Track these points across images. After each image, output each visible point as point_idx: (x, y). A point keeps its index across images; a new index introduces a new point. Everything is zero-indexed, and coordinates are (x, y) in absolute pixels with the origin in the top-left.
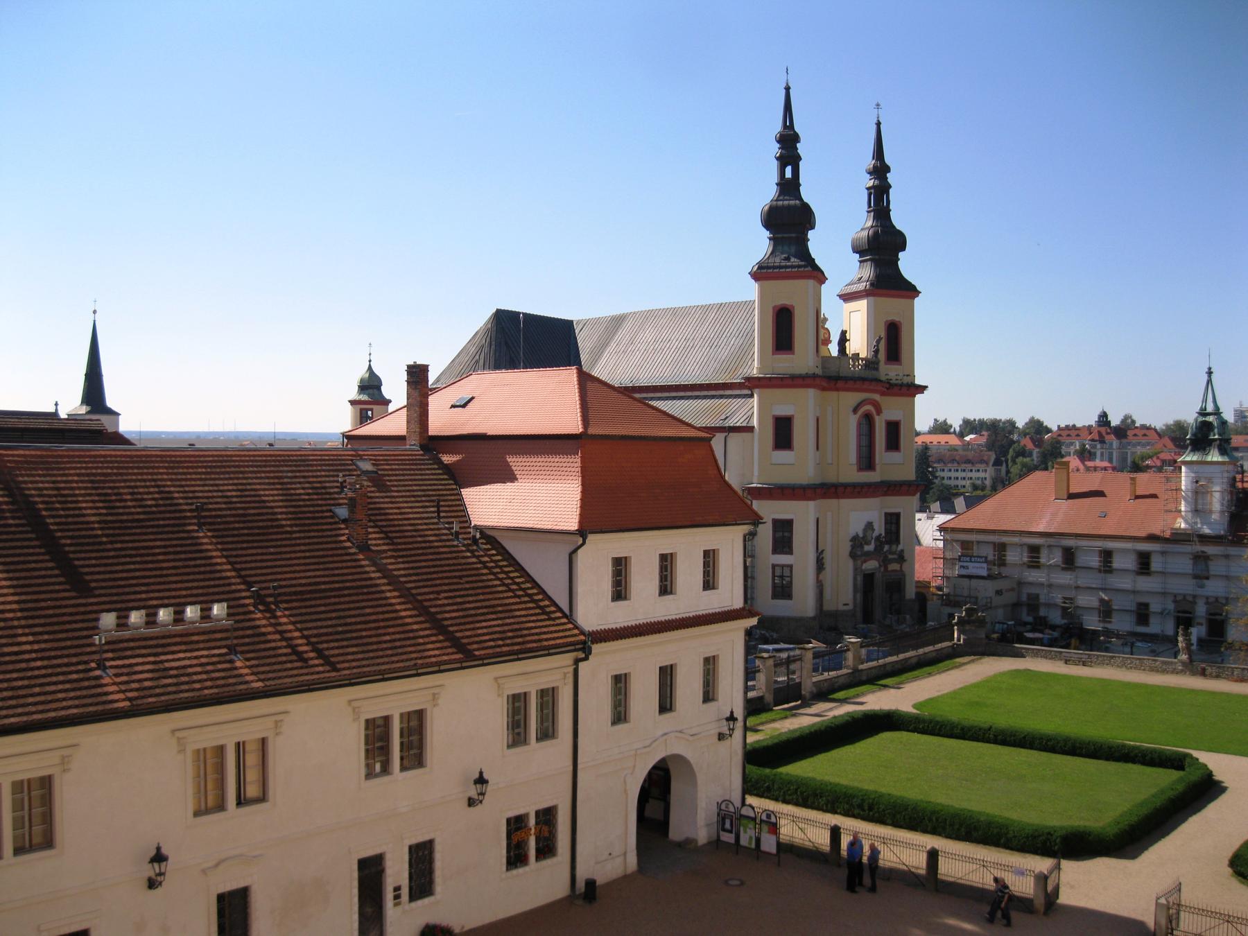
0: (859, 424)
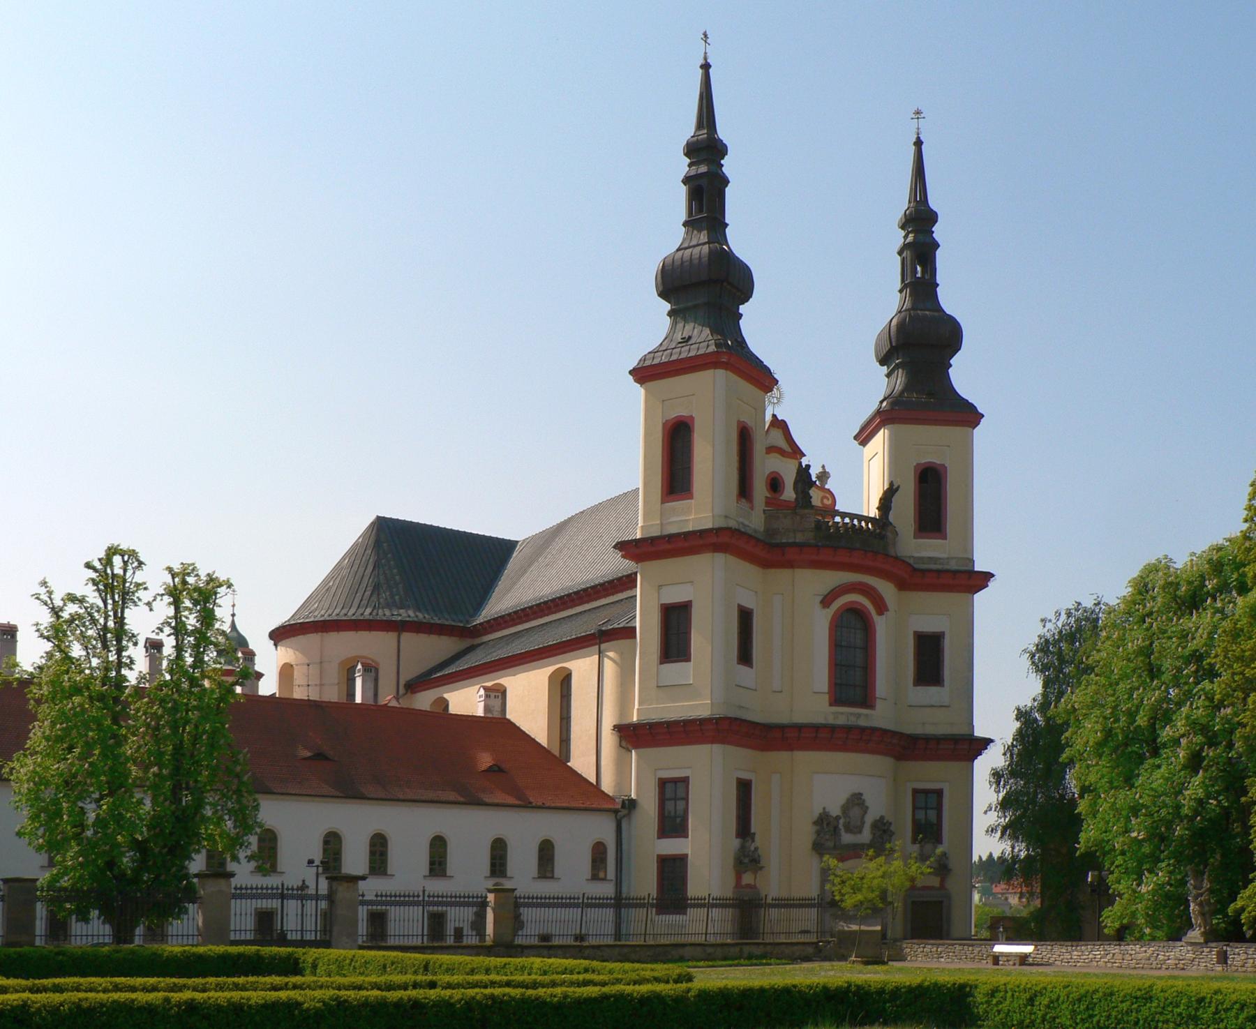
0: (837, 625)
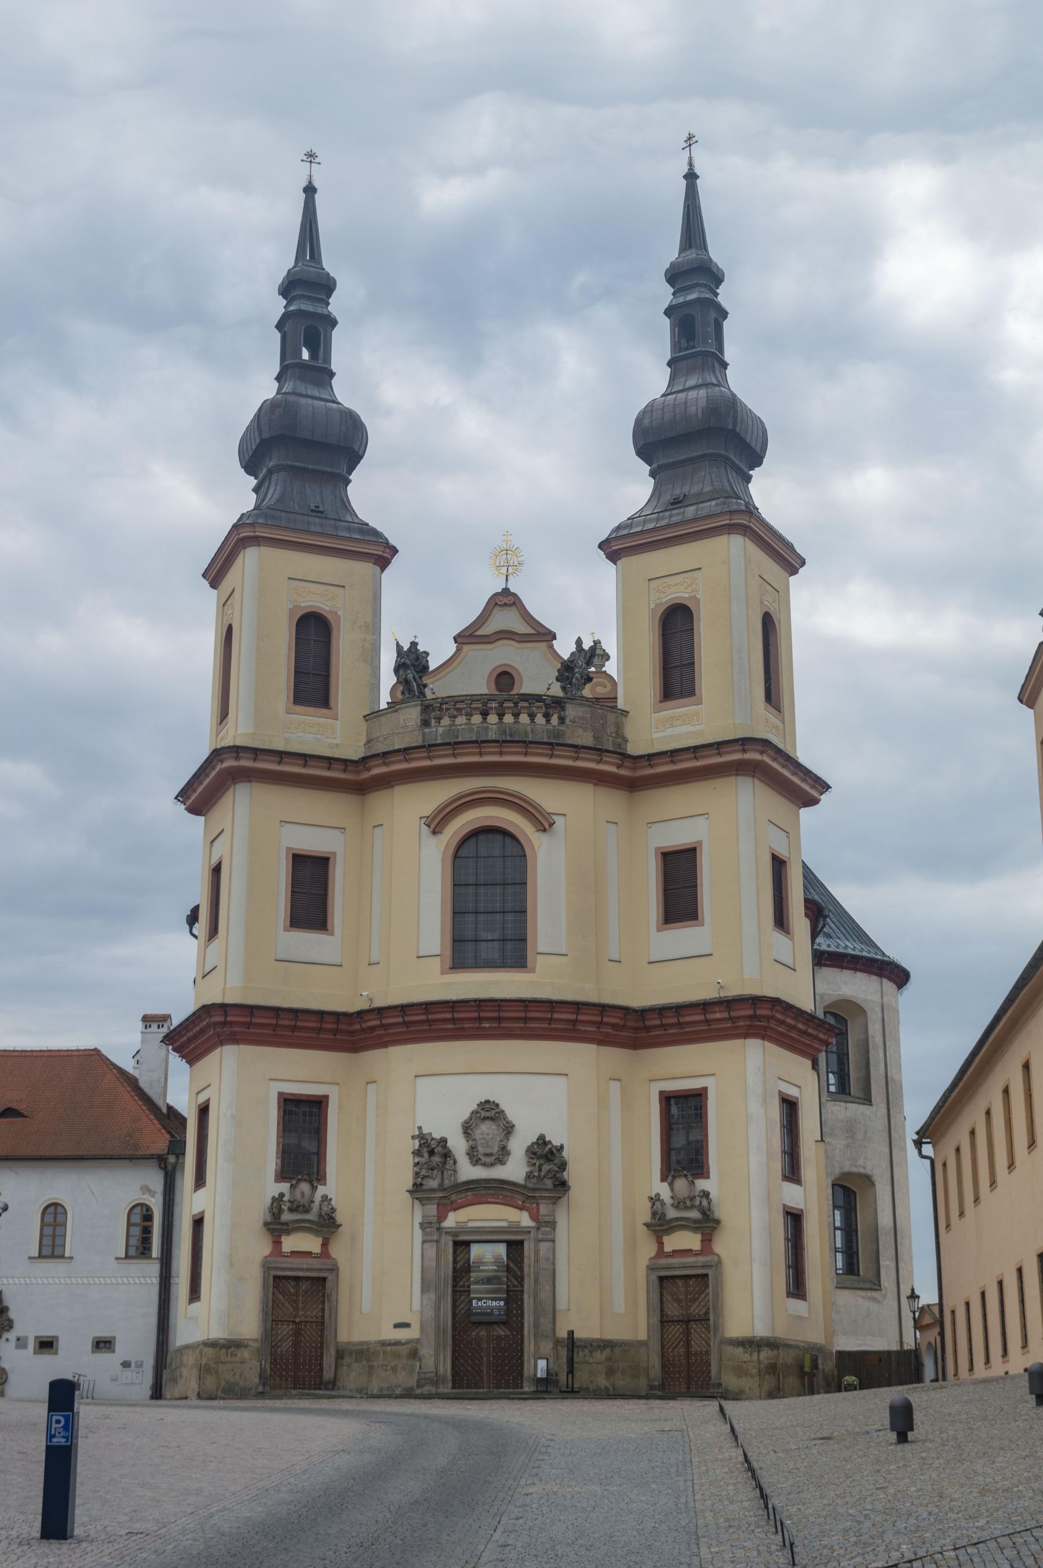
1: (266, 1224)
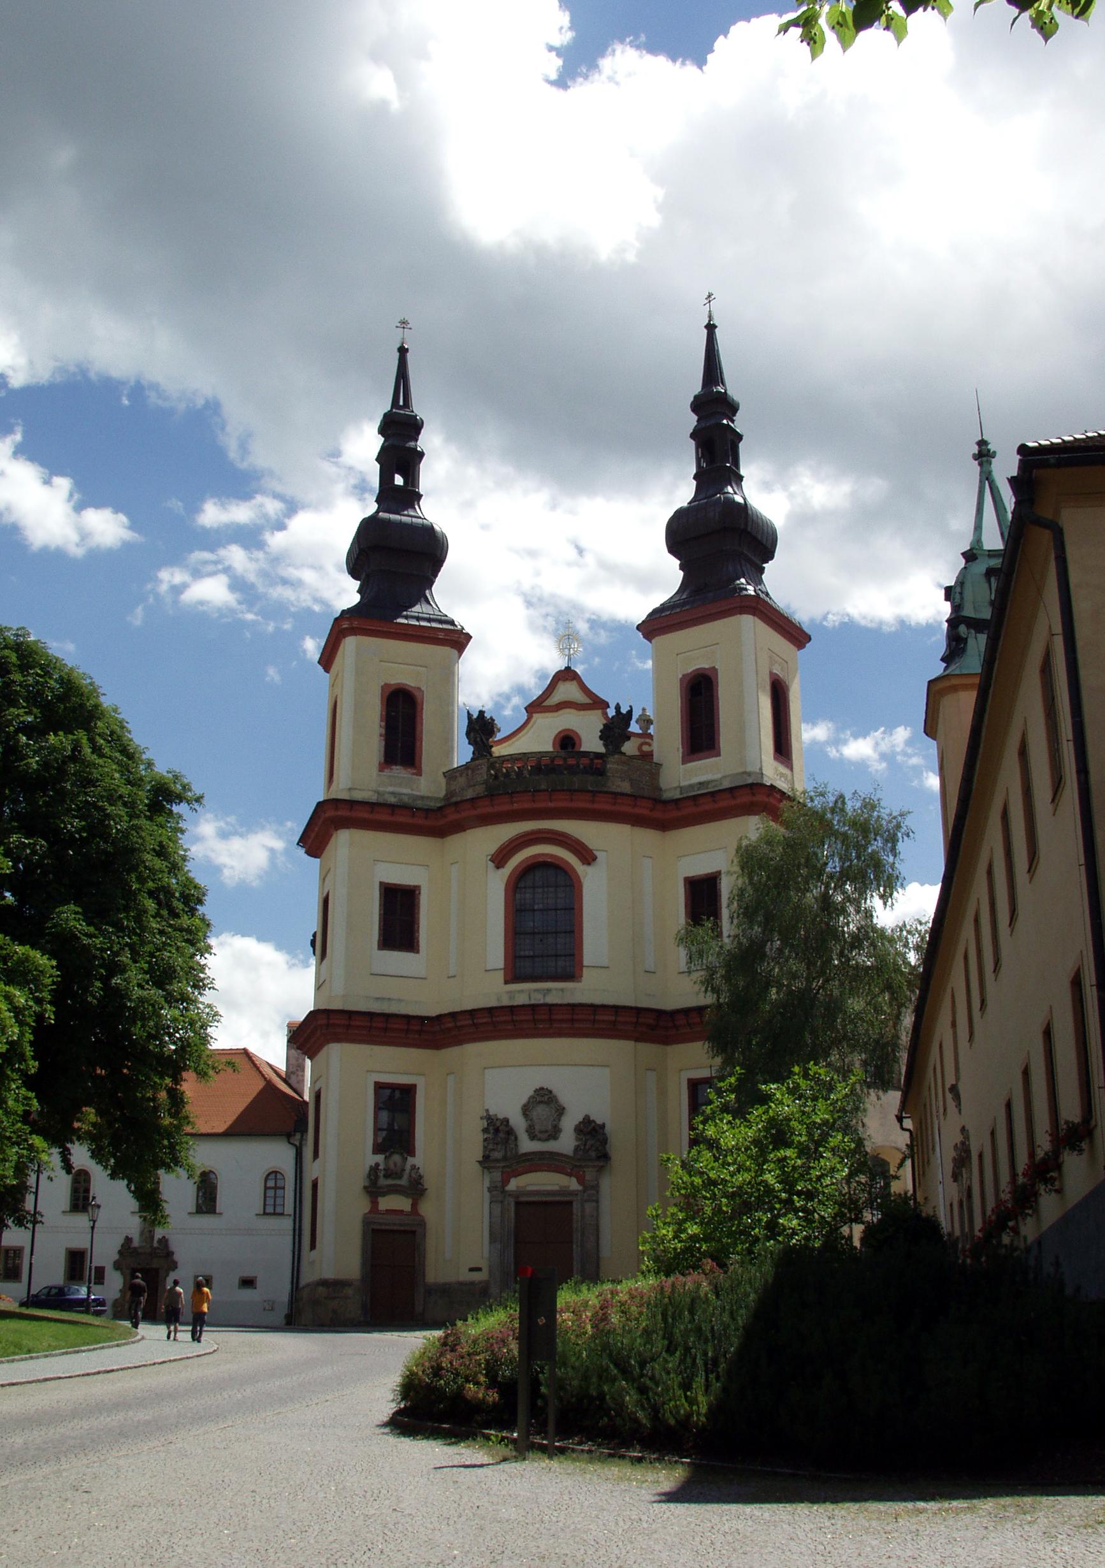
0: (515, 885)
1: (365, 1187)
